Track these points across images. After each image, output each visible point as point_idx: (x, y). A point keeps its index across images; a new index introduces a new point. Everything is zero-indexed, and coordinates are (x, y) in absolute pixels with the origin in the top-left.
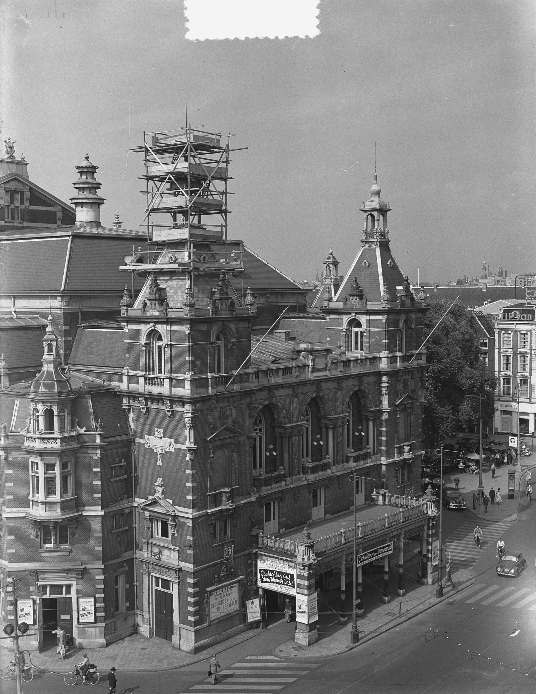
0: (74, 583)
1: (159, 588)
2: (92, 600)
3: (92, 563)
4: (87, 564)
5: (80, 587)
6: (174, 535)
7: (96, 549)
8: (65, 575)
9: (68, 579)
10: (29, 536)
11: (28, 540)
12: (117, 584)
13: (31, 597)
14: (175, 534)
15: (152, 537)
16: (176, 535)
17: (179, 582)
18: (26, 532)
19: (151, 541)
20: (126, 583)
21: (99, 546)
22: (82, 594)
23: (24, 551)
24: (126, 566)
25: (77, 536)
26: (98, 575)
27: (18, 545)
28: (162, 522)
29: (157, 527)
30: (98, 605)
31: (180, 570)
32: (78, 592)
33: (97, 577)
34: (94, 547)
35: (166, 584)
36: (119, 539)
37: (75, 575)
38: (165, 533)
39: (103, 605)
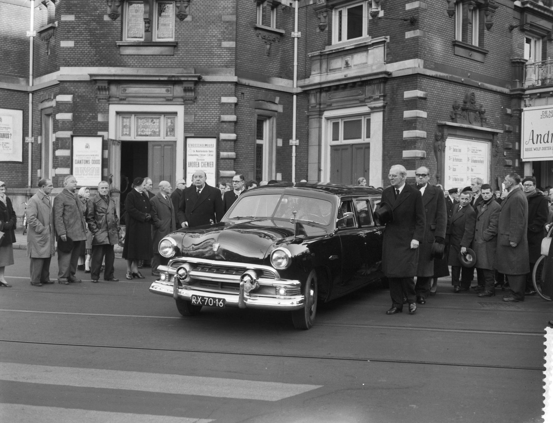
0: (180, 109)
1: (341, 141)
2: (213, 141)
3: (214, 73)
4: (207, 73)
5: (191, 119)
6: (374, 15)
7: (225, 44)
8: (161, 91)
9: (169, 100)
10: (101, 17)
11: (98, 23)
12: (260, 135)
13: (100, 133)
14: (378, 13)
15: (330, 43)
16: (381, 14)
17: (384, 107)
18: (96, 9)
19: (328, 49)
20: (279, 136)
21: (230, 40)
22: (194, 131)
23: (91, 44)
24: (280, 103)
25: (189, 18)
26: (225, 95)
27: (81, 33)
28: (350, 12)
29: (339, 22)
30: (223, 154)
31: (386, 79)
32: (187, 127)
33: (224, 100)
34: (220, 41)
35: (353, 127)
36: (268, 46)
37: (182, 94)
38: (355, 30)
39: (232, 154)
